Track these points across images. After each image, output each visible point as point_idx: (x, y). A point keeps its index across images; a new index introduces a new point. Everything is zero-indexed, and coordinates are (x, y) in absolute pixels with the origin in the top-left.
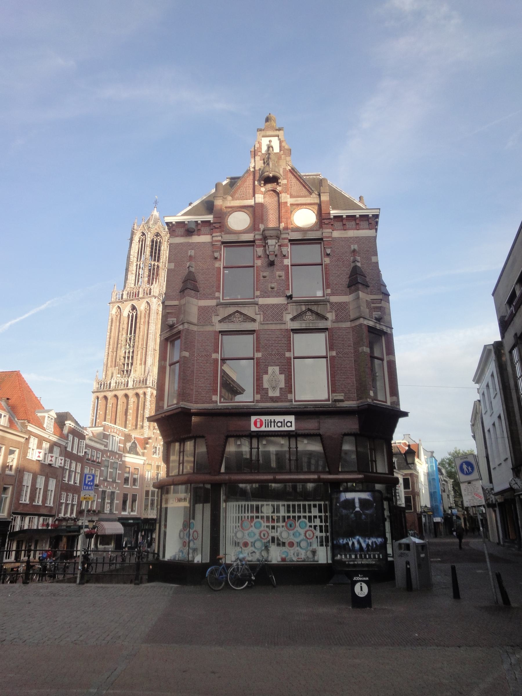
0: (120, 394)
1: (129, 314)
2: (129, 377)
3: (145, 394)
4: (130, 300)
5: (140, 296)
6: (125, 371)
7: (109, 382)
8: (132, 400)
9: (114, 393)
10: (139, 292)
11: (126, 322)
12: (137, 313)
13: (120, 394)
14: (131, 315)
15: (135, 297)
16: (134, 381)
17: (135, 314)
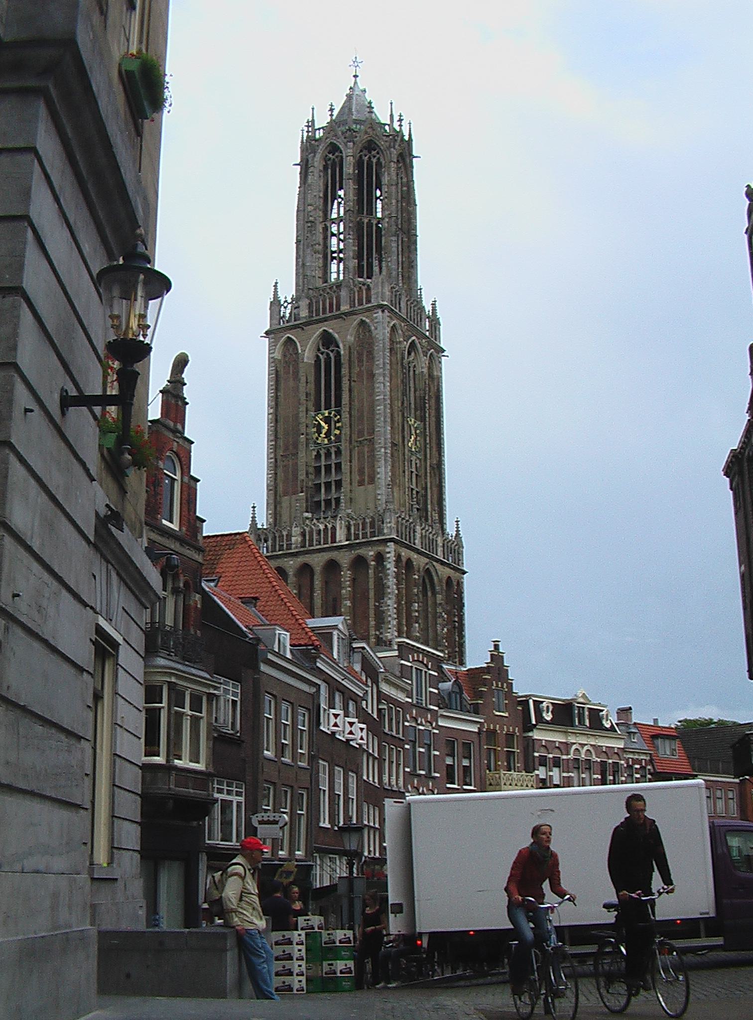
0: (317, 561)
2: (334, 517)
5: (345, 308)
6: (323, 503)
7: (285, 533)
8: (346, 575)
9: (301, 560)
10: (338, 298)
11: (312, 379)
12: (338, 353)
13: (317, 561)
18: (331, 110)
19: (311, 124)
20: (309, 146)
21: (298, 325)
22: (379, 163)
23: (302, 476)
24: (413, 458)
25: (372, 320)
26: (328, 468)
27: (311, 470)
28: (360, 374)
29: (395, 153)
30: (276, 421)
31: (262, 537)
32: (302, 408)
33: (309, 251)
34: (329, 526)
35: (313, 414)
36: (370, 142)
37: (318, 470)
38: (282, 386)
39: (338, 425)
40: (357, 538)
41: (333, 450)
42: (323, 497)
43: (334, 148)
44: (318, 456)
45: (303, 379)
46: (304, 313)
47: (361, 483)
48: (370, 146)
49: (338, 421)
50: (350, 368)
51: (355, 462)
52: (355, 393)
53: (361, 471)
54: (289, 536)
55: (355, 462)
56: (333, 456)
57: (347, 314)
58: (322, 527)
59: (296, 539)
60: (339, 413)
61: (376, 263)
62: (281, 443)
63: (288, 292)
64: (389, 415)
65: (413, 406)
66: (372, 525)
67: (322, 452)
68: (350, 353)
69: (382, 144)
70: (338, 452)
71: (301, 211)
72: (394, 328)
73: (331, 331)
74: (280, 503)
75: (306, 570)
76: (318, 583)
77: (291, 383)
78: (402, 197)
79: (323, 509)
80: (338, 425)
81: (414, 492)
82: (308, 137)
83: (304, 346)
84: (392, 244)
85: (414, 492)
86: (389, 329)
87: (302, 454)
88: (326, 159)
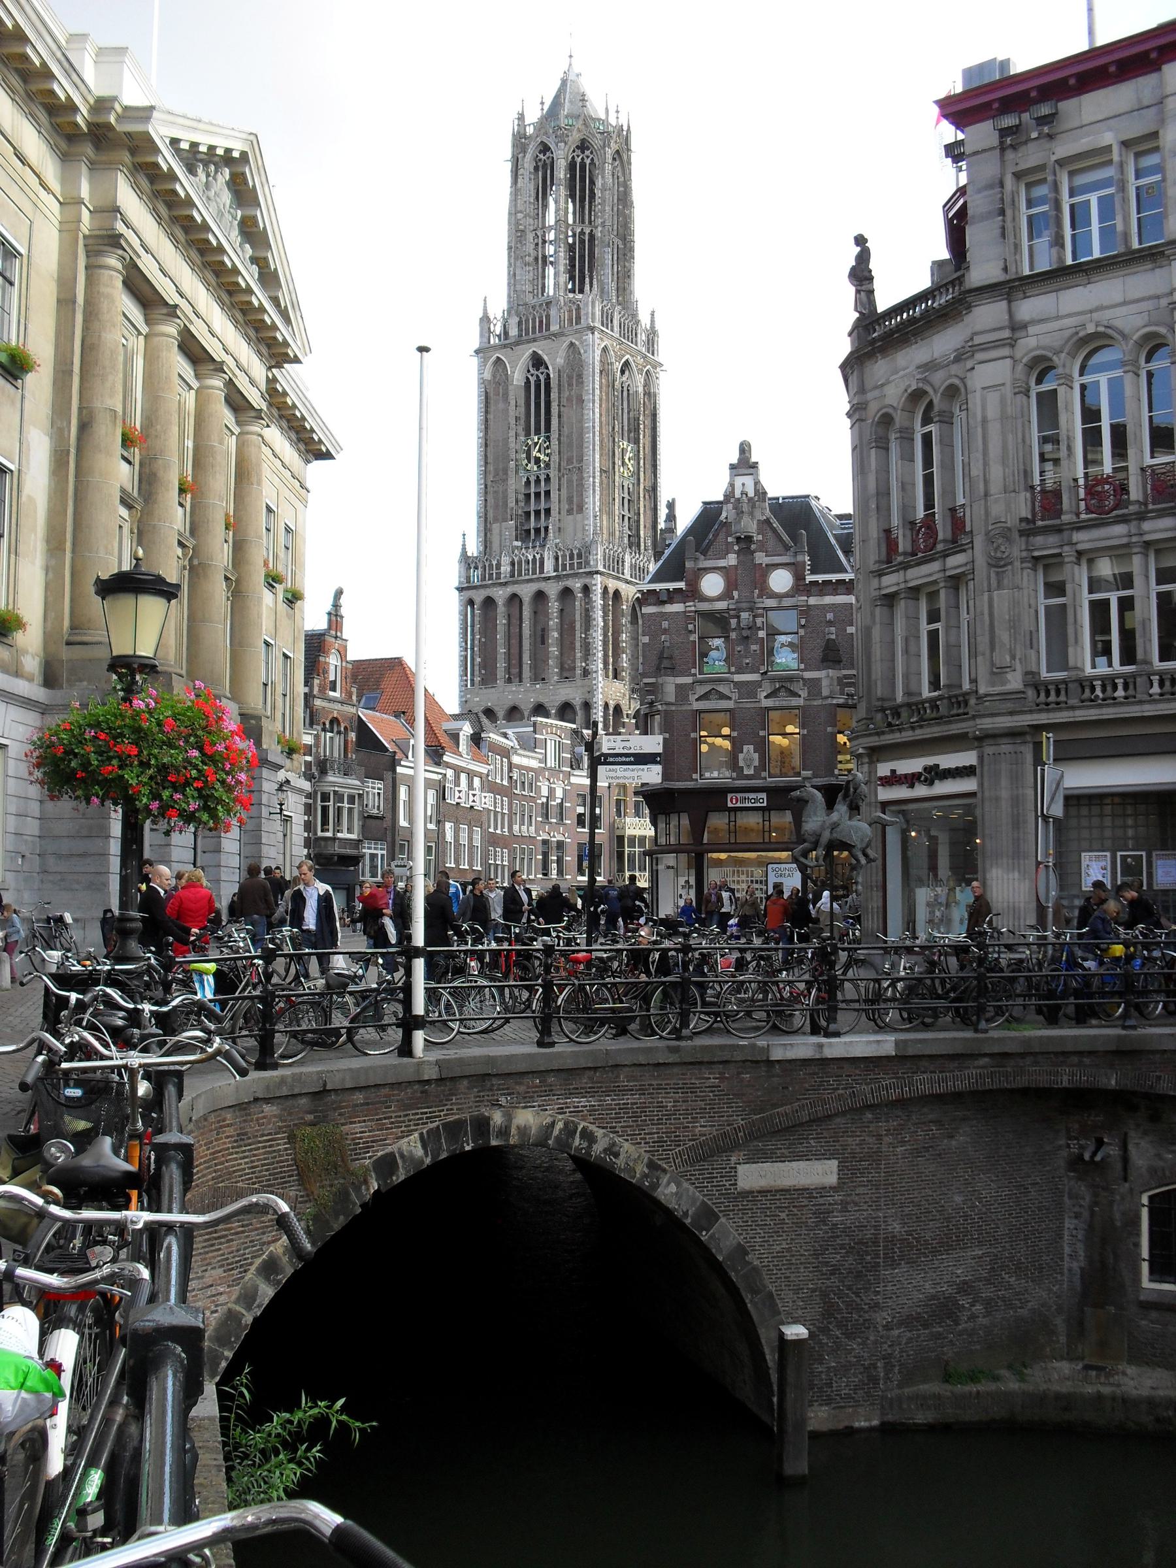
1: (528, 378)
3: (586, 589)
4: (528, 342)
5: (554, 328)
6: (532, 532)
7: (494, 563)
8: (554, 606)
9: (510, 590)
10: (548, 317)
11: (522, 402)
12: (548, 375)
13: (526, 592)
14: (532, 379)
15: (541, 330)
16: (557, 559)
17: (542, 378)
18: (542, 103)
19: (521, 117)
20: (520, 141)
21: (508, 342)
22: (592, 162)
23: (512, 503)
24: (625, 485)
25: (582, 343)
26: (538, 495)
27: (521, 497)
28: (569, 399)
29: (609, 152)
30: (486, 445)
31: (472, 566)
32: (512, 433)
33: (518, 263)
34: (538, 557)
35: (523, 439)
36: (583, 141)
37: (528, 496)
38: (492, 408)
39: (548, 451)
40: (564, 569)
41: (542, 478)
42: (533, 524)
43: (545, 148)
44: (528, 482)
45: (513, 403)
46: (513, 332)
47: (570, 512)
48: (583, 146)
49: (548, 448)
50: (559, 393)
51: (564, 491)
52: (564, 419)
53: (570, 500)
54: (499, 566)
55: (564, 491)
56: (543, 483)
57: (555, 335)
58: (530, 558)
59: (505, 569)
60: (548, 438)
61: (587, 280)
62: (491, 468)
63: (498, 306)
64: (597, 443)
65: (626, 428)
66: (580, 556)
67: (532, 479)
68: (559, 376)
69: (596, 142)
70: (548, 479)
71: (514, 212)
72: (605, 349)
73: (540, 352)
74: (490, 530)
75: (514, 598)
76: (527, 613)
77: (501, 405)
78: (618, 200)
79: (532, 536)
80: (548, 451)
81: (626, 519)
82: (519, 132)
83: (514, 367)
84: (606, 257)
85: (626, 519)
86: (598, 352)
87: (512, 481)
88: (536, 159)
